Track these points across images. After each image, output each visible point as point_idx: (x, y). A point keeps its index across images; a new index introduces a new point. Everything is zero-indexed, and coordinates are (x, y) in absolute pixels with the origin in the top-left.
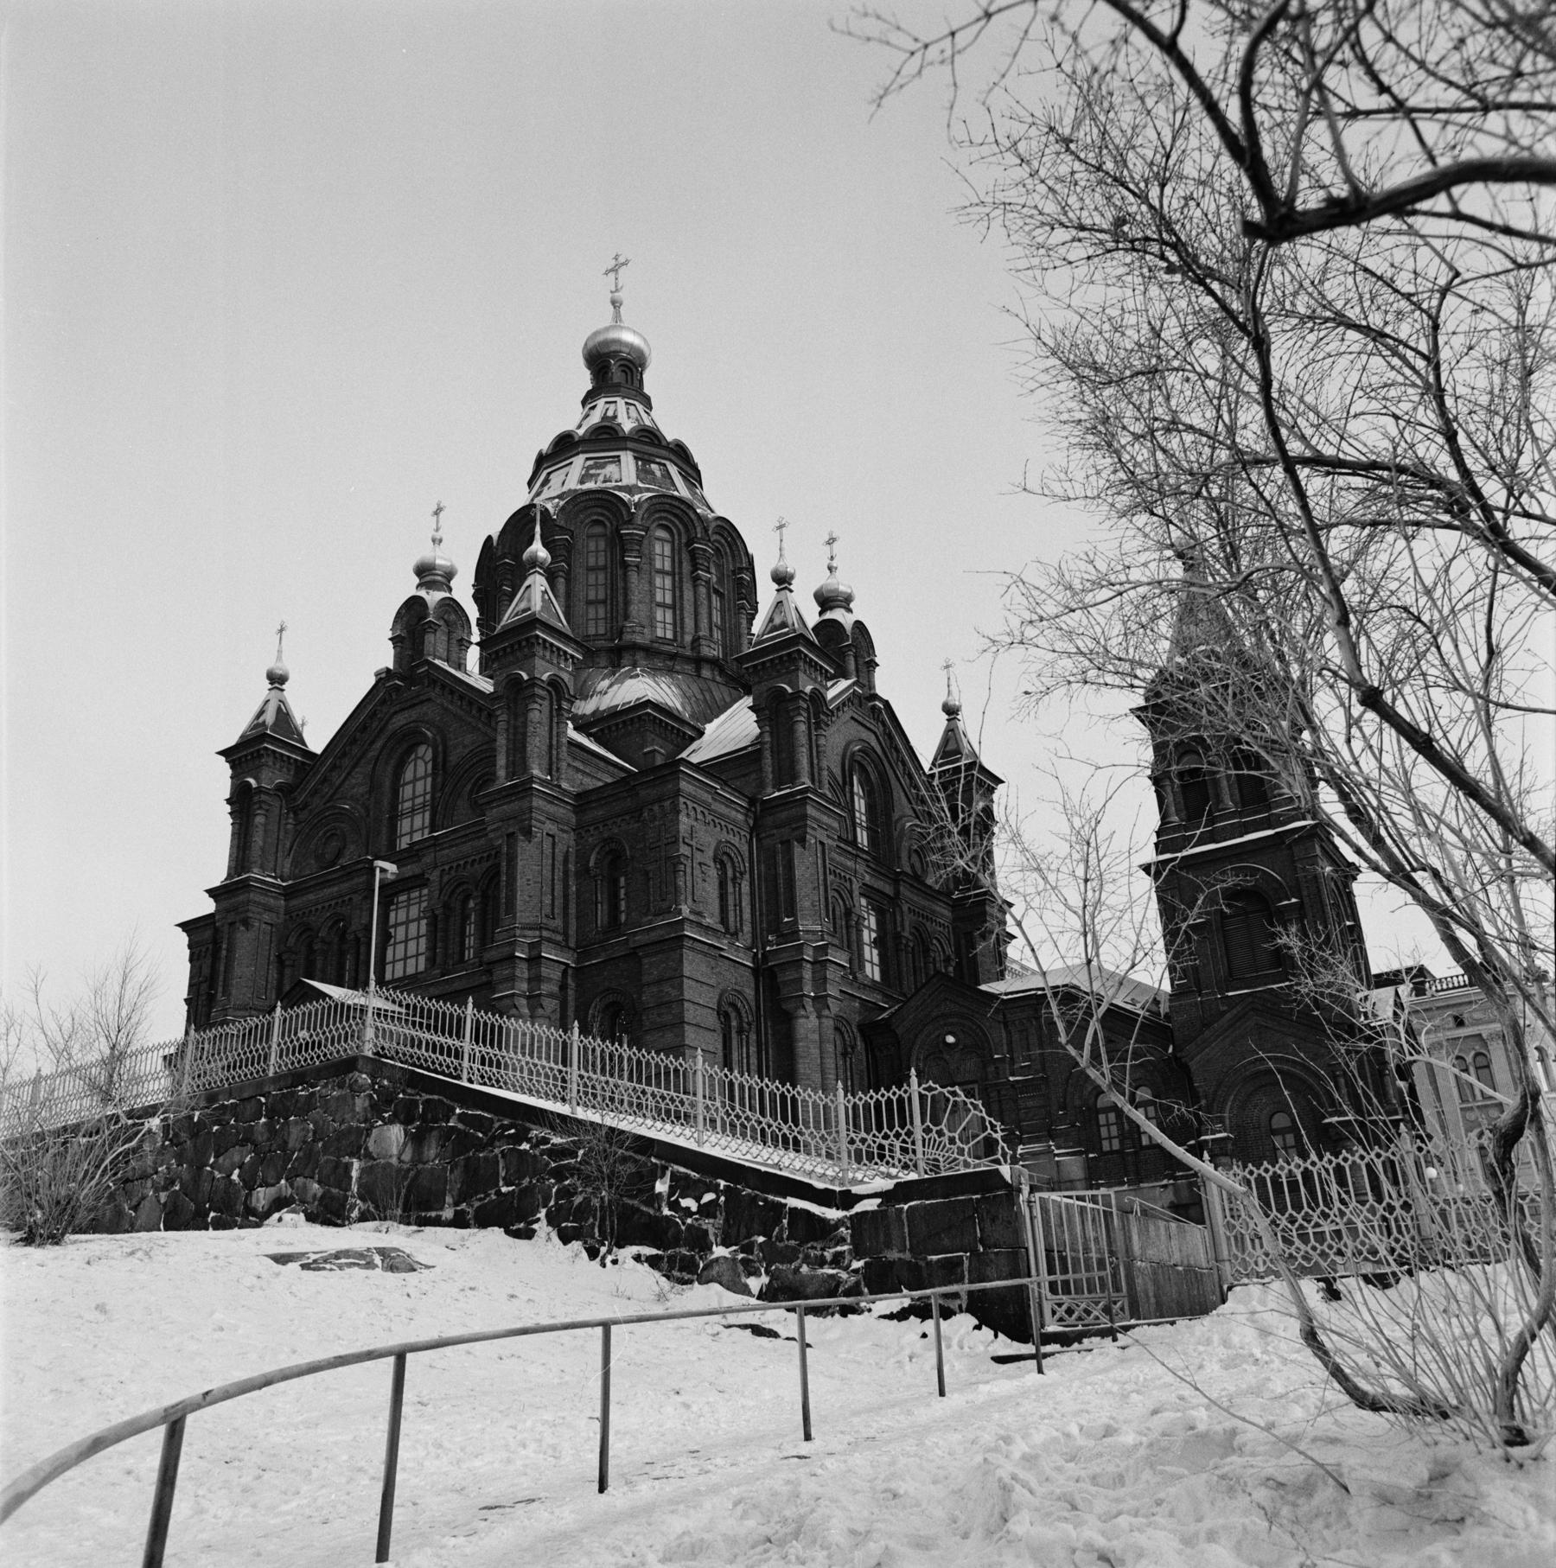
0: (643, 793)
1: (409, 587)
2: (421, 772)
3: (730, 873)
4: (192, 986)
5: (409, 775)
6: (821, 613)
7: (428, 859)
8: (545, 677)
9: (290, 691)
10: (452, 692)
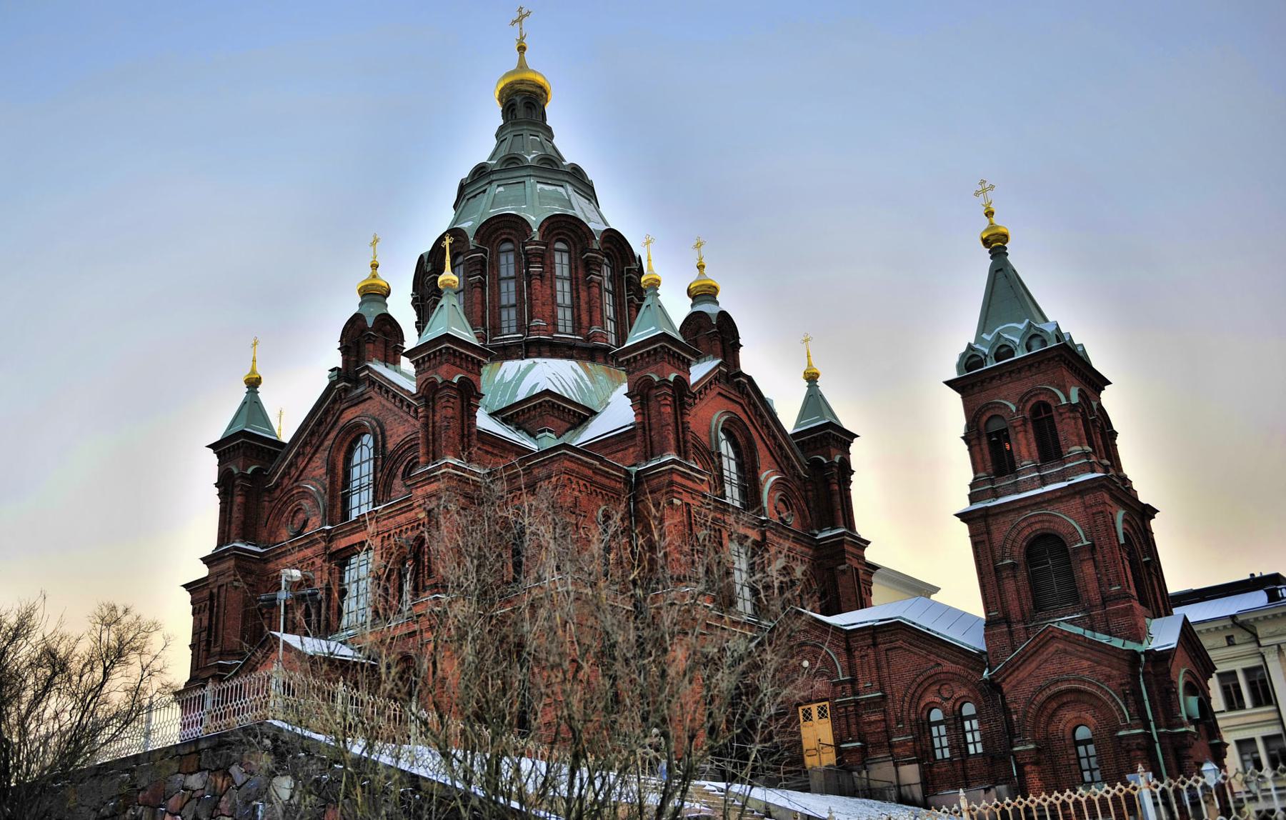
1: (351, 305)
2: (365, 457)
4: (196, 633)
5: (356, 459)
6: (692, 306)
8: (455, 380)
9: (262, 391)
10: (387, 392)
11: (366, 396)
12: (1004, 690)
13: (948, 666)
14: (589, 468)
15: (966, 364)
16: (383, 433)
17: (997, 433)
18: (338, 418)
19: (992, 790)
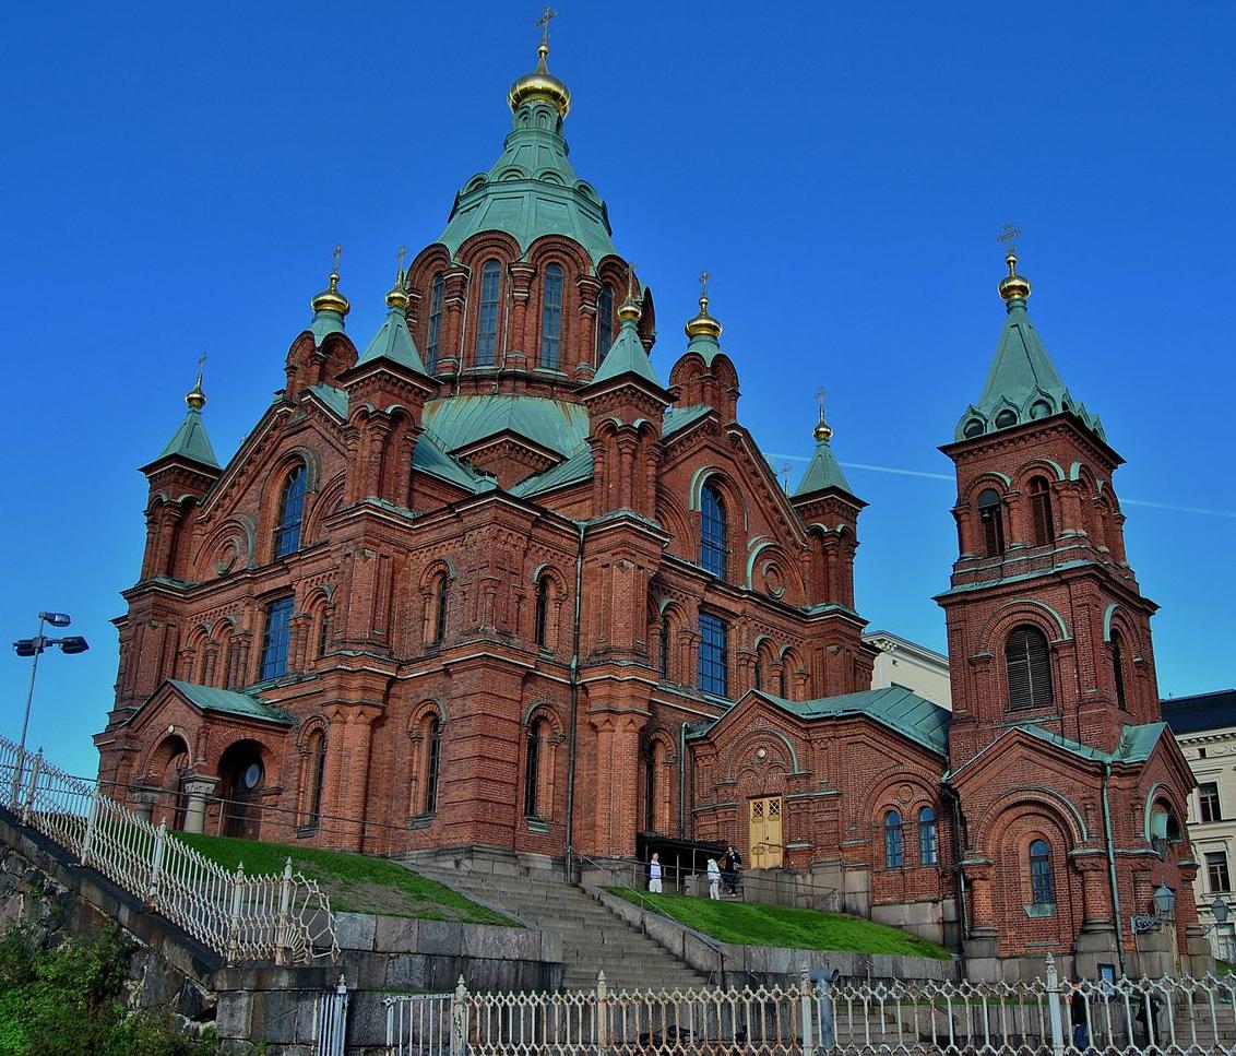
0: (466, 520)
3: (552, 592)
7: (294, 572)
8: (389, 411)
11: (306, 425)
12: (961, 796)
13: (910, 766)
14: (527, 520)
15: (965, 429)
16: (318, 468)
17: (991, 509)
18: (277, 446)
19: (940, 903)
